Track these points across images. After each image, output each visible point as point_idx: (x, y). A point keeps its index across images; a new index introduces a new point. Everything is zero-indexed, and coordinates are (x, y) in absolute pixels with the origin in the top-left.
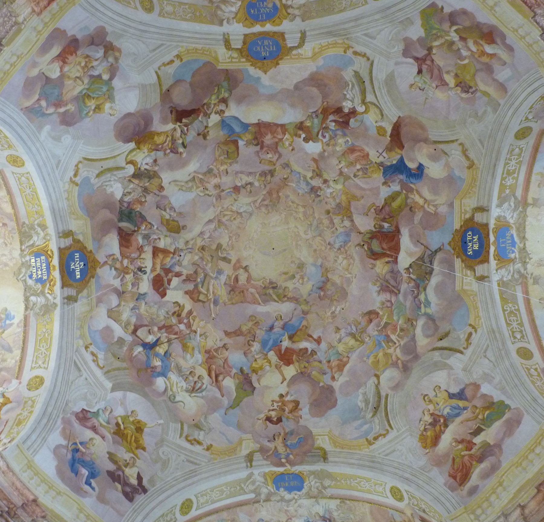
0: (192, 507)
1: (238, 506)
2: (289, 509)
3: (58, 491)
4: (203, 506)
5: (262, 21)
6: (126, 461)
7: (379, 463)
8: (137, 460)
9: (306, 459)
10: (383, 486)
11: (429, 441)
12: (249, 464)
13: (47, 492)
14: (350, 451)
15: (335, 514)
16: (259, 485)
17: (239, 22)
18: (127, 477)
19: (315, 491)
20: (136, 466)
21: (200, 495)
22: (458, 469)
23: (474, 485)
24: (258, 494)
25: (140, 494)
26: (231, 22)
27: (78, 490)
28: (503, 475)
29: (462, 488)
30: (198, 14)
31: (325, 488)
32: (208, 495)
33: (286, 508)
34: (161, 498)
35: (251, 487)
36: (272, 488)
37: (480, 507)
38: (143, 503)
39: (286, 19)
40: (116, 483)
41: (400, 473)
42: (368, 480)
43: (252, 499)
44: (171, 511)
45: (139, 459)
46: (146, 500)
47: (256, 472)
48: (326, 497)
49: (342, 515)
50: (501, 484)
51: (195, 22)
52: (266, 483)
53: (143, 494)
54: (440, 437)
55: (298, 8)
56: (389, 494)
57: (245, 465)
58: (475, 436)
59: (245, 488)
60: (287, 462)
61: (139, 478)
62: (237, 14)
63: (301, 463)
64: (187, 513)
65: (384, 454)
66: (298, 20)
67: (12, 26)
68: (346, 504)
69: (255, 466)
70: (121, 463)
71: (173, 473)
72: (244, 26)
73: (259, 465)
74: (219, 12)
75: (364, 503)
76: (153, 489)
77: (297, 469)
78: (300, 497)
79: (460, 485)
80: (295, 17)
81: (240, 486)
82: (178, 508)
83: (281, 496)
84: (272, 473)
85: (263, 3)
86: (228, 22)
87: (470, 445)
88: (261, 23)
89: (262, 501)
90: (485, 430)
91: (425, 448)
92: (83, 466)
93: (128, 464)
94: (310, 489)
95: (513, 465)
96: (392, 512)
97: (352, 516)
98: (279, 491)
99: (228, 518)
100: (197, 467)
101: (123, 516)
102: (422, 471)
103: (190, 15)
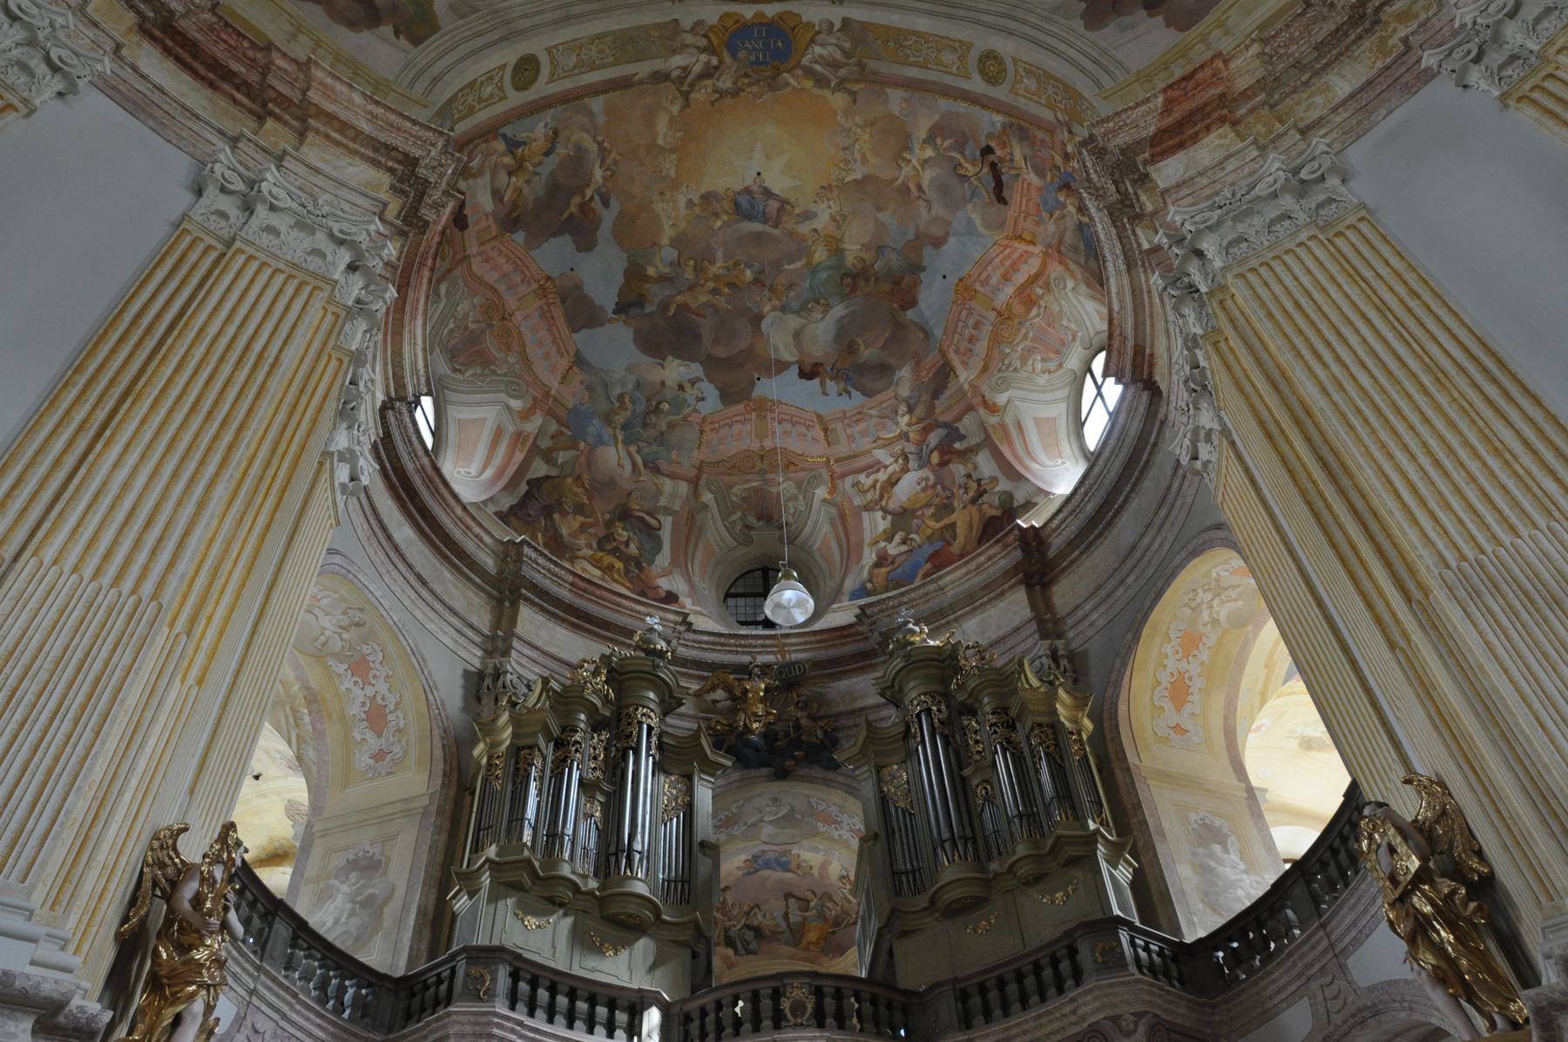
5: (761, 24)
17: (810, 25)
26: (825, 26)
30: (891, 44)
39: (712, 27)
51: (900, 29)
55: (687, 46)
62: (812, 41)
66: (687, 23)
67: (1274, 37)
72: (800, 16)
74: (847, 45)
80: (692, 29)
85: (757, 58)
86: (831, 24)
88: (764, 21)
103: (907, 43)
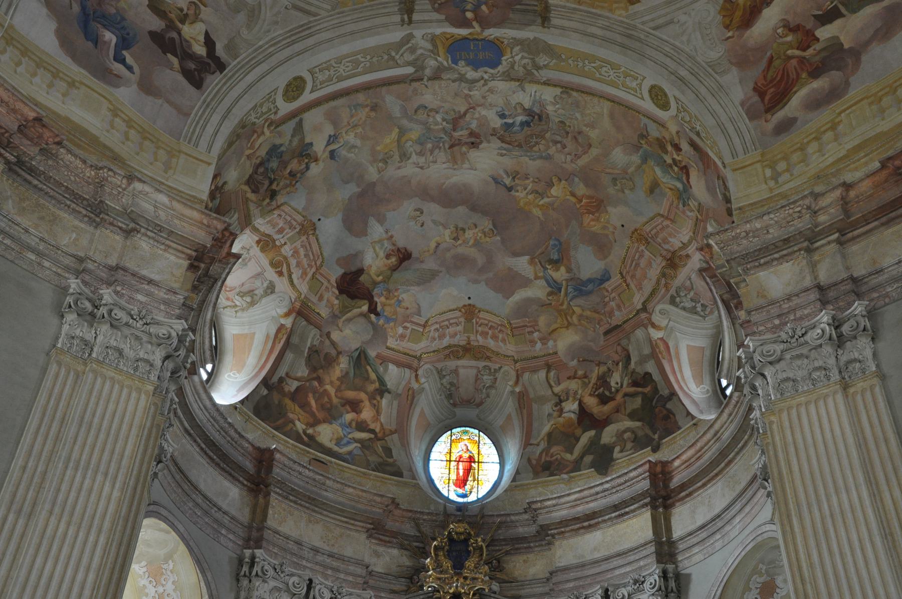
0: (303, 89)
1: (384, 85)
2: (471, 93)
3: (69, 80)
4: (323, 86)
6: (181, 10)
7: (639, 40)
8: (202, 7)
9: (511, 16)
10: (639, 81)
11: (738, 14)
12: (406, 17)
13: (51, 86)
14: (594, 10)
15: (550, 109)
16: (422, 54)
18: (187, 41)
19: (520, 71)
20: (202, 21)
21: (317, 70)
22: (771, 81)
23: (790, 115)
24: (420, 68)
25: (213, 73)
27: (105, 75)
28: (844, 111)
29: (769, 116)
31: (538, 68)
32: (332, 70)
33: (466, 92)
34: (250, 78)
35: (409, 57)
36: (443, 60)
37: (786, 158)
38: (221, 87)
40: (169, 55)
41: (672, 65)
42: (614, 66)
43: (407, 76)
44: (270, 97)
45: (205, 6)
46: (225, 84)
47: (418, 33)
48: (538, 82)
49: (560, 111)
50: (834, 127)
52: (435, 52)
53: (218, 72)
54: (760, 12)
56: (646, 95)
57: (397, 18)
58: (823, 24)
59: (397, 57)
60: (476, 19)
61: (209, 43)
63: (500, 24)
64: (295, 98)
65: (652, 24)
68: (570, 96)
69: (418, 22)
70: (173, 16)
71: (269, 31)
73: (424, 21)
75: (602, 100)
76: (235, 63)
77: (492, 33)
78: (493, 78)
79: (767, 111)
81: (389, 55)
82: (280, 92)
83: (459, 74)
84: (448, 36)
87: (807, 38)
89: (426, 78)
90: (842, 16)
91: (727, 27)
92: (105, 26)
93: (186, 15)
94: (512, 67)
95: (867, 98)
96: (645, 120)
97: (578, 115)
98: (456, 64)
99: (366, 103)
100: (312, 19)
101: (187, 115)
102: (710, 70)
